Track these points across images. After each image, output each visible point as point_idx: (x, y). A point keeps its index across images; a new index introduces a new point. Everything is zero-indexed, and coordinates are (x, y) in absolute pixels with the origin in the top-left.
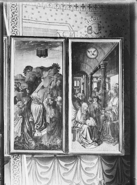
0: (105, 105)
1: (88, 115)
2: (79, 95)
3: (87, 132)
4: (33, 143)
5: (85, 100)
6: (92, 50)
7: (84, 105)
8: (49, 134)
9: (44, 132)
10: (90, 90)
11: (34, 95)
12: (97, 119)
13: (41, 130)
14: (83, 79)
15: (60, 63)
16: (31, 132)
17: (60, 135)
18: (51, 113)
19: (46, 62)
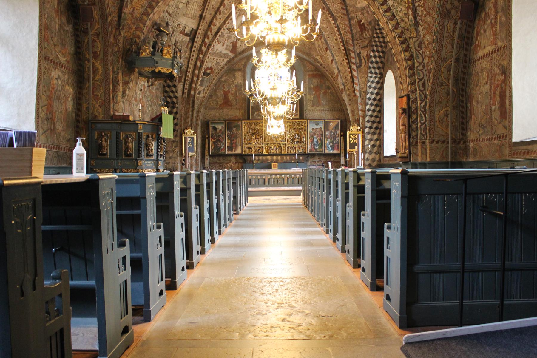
0: (335, 139)
1: (330, 142)
2: (328, 137)
3: (330, 147)
4: (315, 151)
5: (329, 138)
6: (331, 123)
7: (329, 139)
8: (319, 148)
9: (318, 147)
10: (331, 135)
11: (315, 136)
12: (333, 143)
13: (317, 147)
14: (329, 132)
15: (322, 127)
16: (314, 147)
17: (322, 148)
18: (320, 142)
19: (318, 127)
